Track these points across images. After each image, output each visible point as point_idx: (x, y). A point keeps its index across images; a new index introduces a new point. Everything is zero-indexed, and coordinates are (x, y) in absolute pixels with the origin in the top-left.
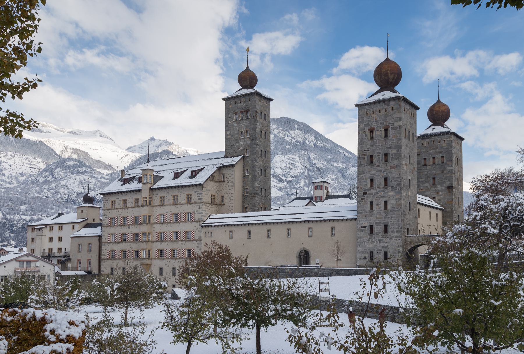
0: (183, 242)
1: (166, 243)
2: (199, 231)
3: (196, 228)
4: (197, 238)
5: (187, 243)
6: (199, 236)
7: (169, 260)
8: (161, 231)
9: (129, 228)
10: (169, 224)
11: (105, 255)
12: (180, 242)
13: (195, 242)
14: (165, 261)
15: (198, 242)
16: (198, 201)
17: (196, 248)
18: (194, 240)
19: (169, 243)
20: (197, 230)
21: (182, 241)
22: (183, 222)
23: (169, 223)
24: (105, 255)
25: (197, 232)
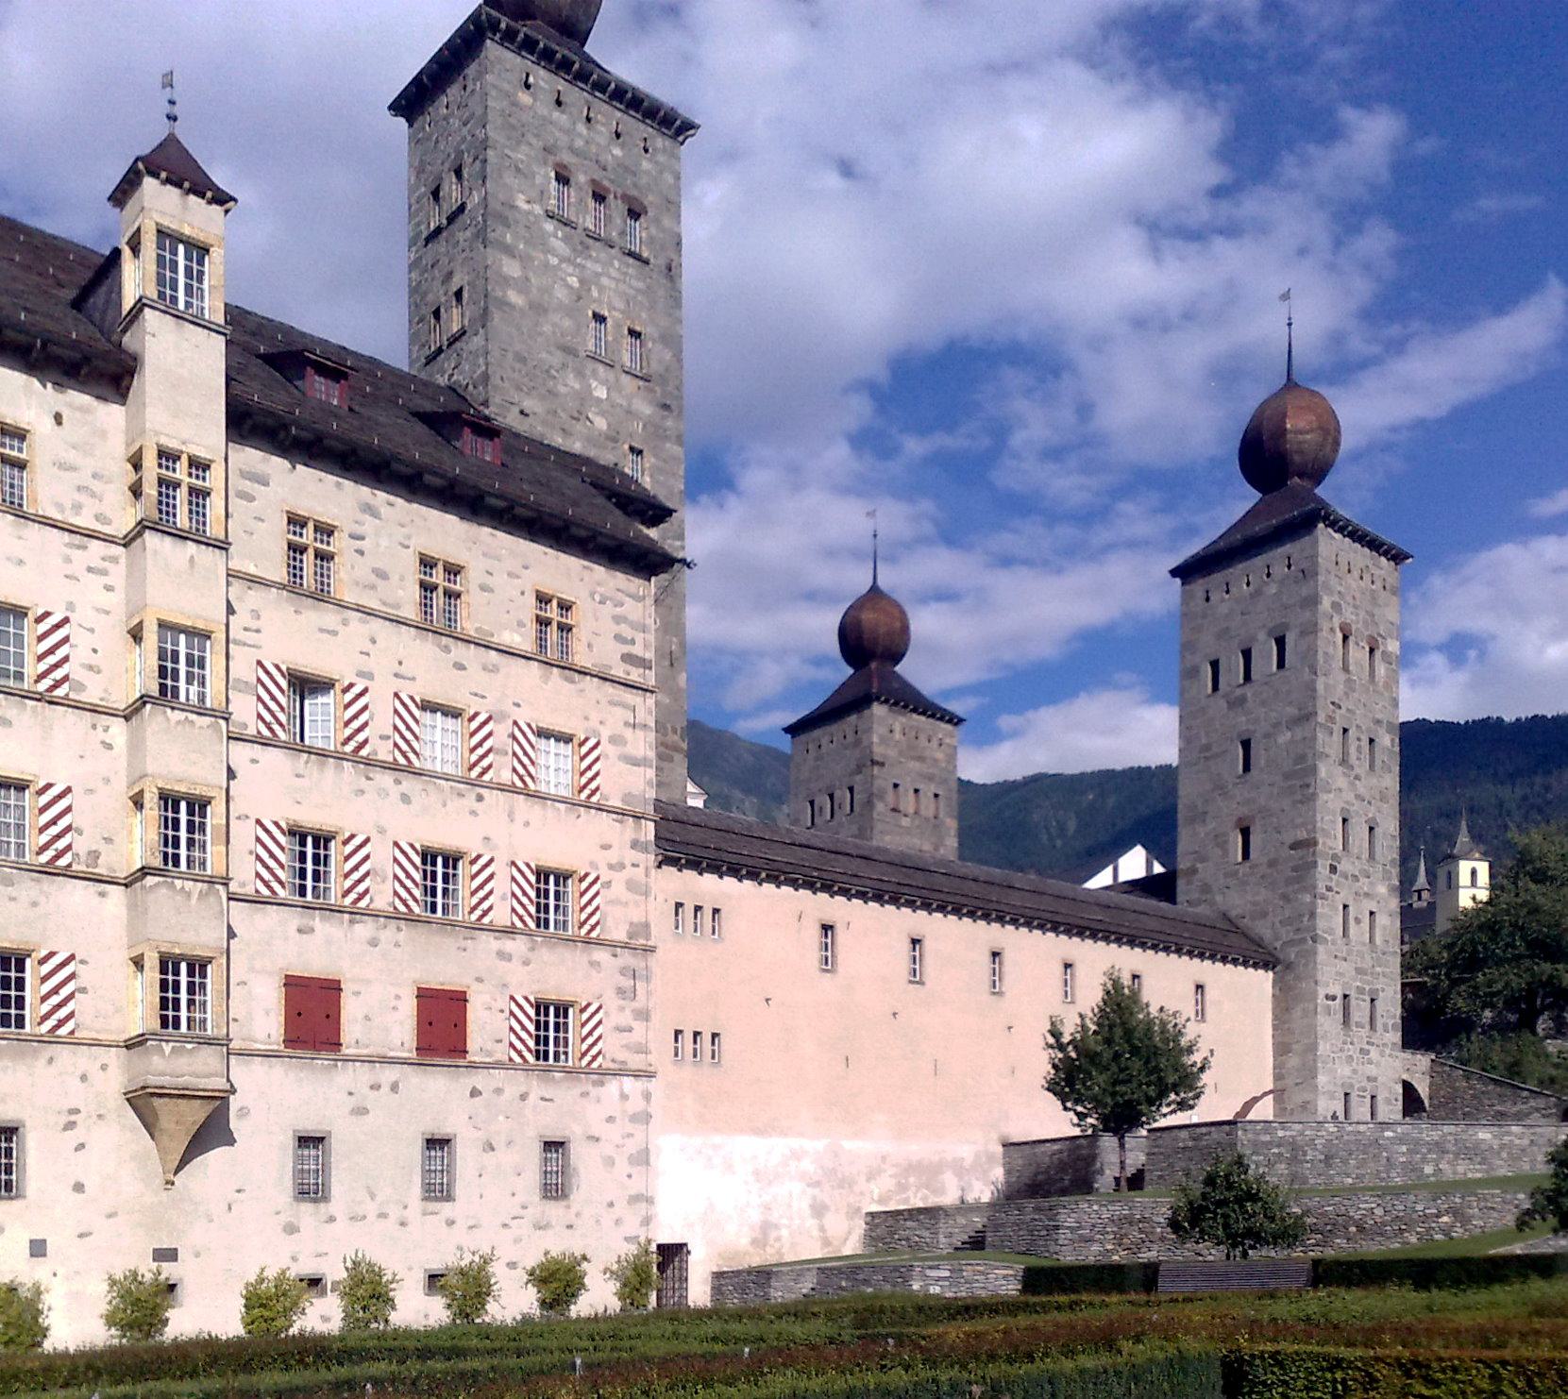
0: (517, 946)
1: (365, 929)
5: (545, 954)
6: (637, 916)
7: (388, 1074)
12: (489, 943)
13: (601, 955)
14: (355, 1077)
15: (626, 958)
16: (619, 671)
17: (611, 1002)
18: (600, 943)
19: (389, 933)
21: (510, 931)
22: (511, 789)
25: (618, 889)
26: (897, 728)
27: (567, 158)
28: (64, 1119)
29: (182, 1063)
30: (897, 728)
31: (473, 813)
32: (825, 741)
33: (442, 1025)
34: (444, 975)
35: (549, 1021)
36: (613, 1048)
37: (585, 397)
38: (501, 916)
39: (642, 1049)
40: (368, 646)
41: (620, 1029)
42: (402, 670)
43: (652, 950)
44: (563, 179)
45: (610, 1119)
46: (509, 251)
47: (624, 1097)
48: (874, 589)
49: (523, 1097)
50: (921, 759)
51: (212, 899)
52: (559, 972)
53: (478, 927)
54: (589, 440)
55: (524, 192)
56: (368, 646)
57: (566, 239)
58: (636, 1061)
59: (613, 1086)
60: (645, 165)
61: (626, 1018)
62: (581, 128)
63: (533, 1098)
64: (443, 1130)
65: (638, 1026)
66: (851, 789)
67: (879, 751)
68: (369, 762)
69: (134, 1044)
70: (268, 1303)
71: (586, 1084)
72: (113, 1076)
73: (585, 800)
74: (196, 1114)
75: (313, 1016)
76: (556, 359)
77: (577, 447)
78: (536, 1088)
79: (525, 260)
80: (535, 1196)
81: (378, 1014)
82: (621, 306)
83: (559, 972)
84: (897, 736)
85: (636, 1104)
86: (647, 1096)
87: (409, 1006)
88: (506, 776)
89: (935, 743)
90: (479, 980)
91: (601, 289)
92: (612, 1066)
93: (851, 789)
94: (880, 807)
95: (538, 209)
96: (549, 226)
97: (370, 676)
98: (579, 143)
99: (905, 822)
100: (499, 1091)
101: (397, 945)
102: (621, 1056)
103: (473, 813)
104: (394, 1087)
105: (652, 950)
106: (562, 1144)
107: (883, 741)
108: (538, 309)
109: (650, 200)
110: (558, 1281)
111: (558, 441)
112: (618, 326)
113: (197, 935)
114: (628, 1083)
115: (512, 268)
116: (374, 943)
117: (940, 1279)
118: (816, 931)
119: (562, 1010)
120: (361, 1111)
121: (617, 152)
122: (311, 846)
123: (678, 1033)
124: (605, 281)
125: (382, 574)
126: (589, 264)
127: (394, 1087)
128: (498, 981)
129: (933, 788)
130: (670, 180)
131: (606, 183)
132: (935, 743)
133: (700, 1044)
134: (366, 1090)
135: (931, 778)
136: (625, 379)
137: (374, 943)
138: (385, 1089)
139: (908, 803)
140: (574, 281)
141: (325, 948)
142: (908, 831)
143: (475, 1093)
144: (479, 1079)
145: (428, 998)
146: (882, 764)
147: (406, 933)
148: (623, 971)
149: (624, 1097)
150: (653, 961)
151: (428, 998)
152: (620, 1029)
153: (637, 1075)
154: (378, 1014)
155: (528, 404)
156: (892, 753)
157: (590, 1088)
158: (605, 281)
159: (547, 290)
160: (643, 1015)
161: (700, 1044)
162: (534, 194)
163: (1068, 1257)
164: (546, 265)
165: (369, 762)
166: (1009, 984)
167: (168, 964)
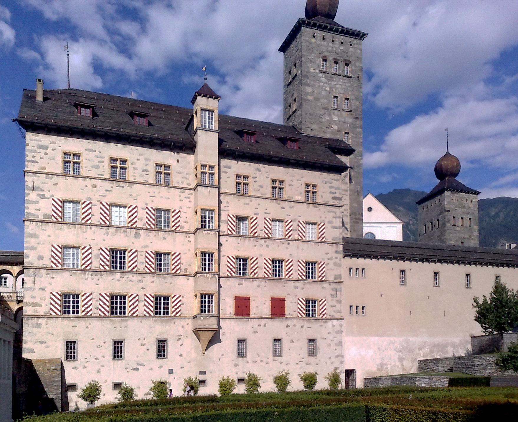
0: (300, 284)
1: (256, 283)
2: (335, 264)
3: (329, 256)
4: (331, 279)
6: (337, 273)
7: (263, 322)
8: (241, 254)
9: (137, 236)
10: (262, 242)
11: (35, 305)
12: (291, 284)
13: (326, 285)
14: (253, 323)
15: (334, 285)
17: (329, 298)
18: (325, 281)
19: (263, 283)
20: (331, 262)
21: (297, 280)
23: (264, 238)
24: (35, 305)
25: (331, 266)
26: (454, 198)
27: (326, 54)
28: (178, 337)
29: (206, 322)
30: (454, 198)
31: (287, 248)
32: (429, 205)
33: (278, 308)
34: (278, 293)
35: (310, 306)
36: (329, 312)
37: (331, 121)
38: (295, 276)
39: (339, 312)
40: (258, 206)
41: (332, 306)
42: (267, 211)
43: (342, 282)
44: (325, 60)
45: (329, 333)
46: (308, 85)
47: (333, 326)
48: (448, 154)
49: (302, 327)
50: (464, 207)
51: (214, 278)
52: (312, 291)
53: (288, 280)
54: (332, 133)
55: (313, 67)
56: (258, 206)
57: (325, 78)
58: (337, 316)
59: (330, 323)
60: (351, 49)
61: (334, 303)
62: (331, 44)
63: (305, 327)
64: (279, 337)
65: (338, 306)
66: (438, 220)
67: (447, 207)
68: (257, 238)
69: (195, 317)
70: (226, 386)
71: (321, 323)
72: (189, 326)
73: (321, 241)
74: (210, 335)
75: (242, 307)
76: (322, 111)
77: (328, 136)
78: (306, 324)
79: (313, 86)
80: (306, 355)
81: (260, 306)
82: (342, 92)
83: (312, 291)
84: (454, 201)
85: (337, 328)
86: (341, 326)
87: (269, 303)
88: (296, 237)
89: (469, 201)
90: (289, 294)
91: (336, 89)
92: (329, 317)
93: (438, 220)
94: (448, 225)
95: (317, 71)
96: (320, 75)
97: (257, 214)
98: (330, 48)
99: (458, 229)
100: (295, 325)
101: (265, 286)
102: (332, 314)
103: (287, 248)
104: (265, 325)
105: (342, 282)
106: (314, 340)
107: (449, 203)
108: (317, 99)
109: (352, 59)
110: (310, 380)
111: (322, 135)
112: (341, 98)
113: (211, 287)
114: (335, 322)
115: (309, 90)
116: (259, 286)
117: (425, 381)
118: (398, 273)
119: (314, 301)
120: (256, 332)
121: (342, 48)
122: (242, 261)
123: (351, 307)
124: (338, 86)
125: (261, 187)
126: (333, 83)
127: (265, 325)
128: (294, 295)
129: (469, 217)
130: (358, 51)
131: (338, 58)
132: (469, 201)
133: (358, 309)
134: (257, 326)
135: (468, 213)
136: (344, 113)
137: (259, 286)
138: (262, 326)
139: (459, 222)
140: (328, 89)
141: (244, 288)
142: (459, 232)
143: (288, 326)
144: (289, 322)
145: (274, 300)
146: (449, 211)
147: (268, 283)
148: (333, 289)
149: (333, 326)
150: (342, 286)
151: (273, 300)
152: (332, 306)
153: (337, 319)
154: (260, 306)
155: (313, 127)
156: (453, 207)
157: (322, 324)
158: (338, 86)
159: (320, 93)
160: (339, 302)
161: (358, 309)
162: (316, 67)
163: (478, 374)
164: (319, 86)
165: (257, 238)
166: (472, 285)
167: (203, 296)
